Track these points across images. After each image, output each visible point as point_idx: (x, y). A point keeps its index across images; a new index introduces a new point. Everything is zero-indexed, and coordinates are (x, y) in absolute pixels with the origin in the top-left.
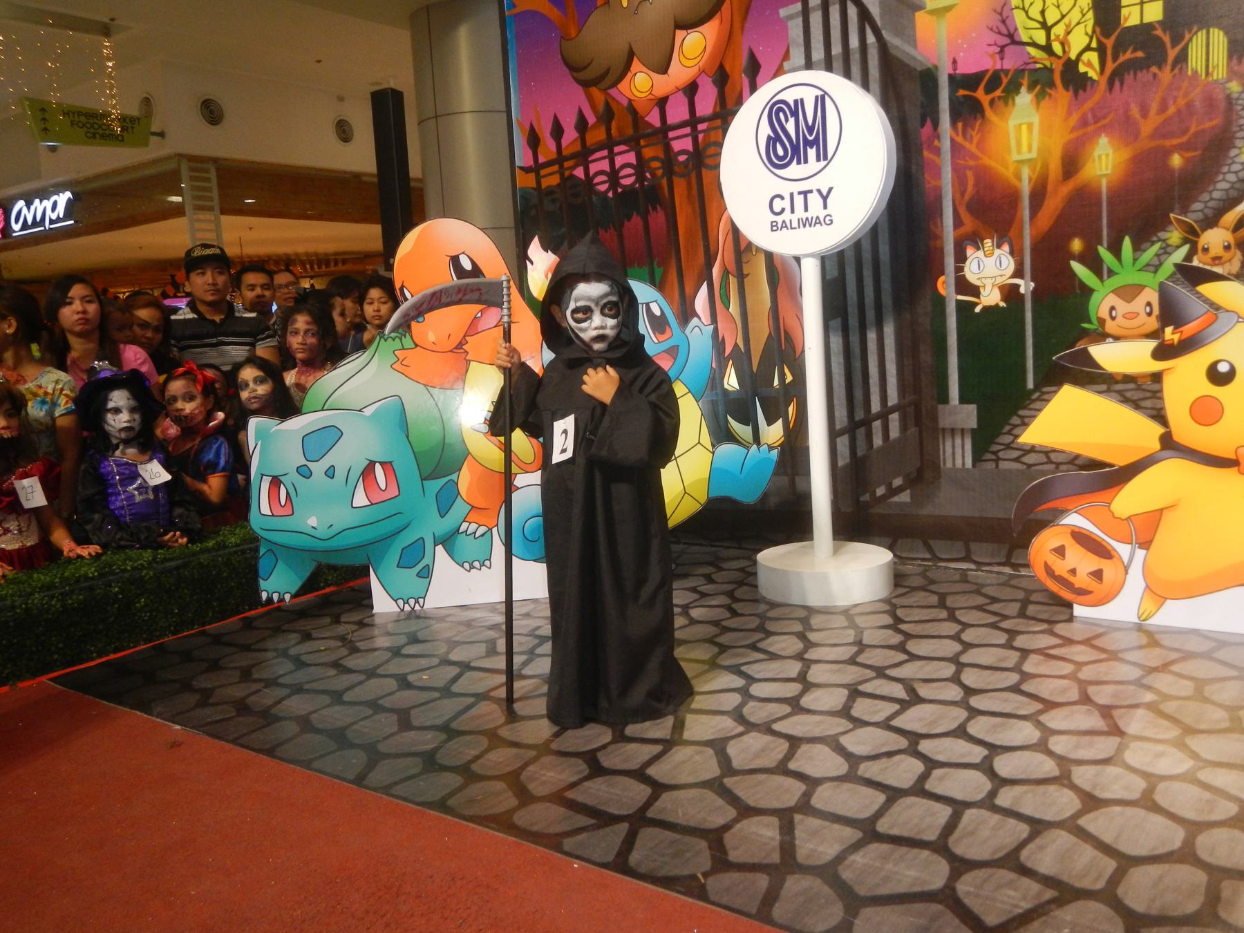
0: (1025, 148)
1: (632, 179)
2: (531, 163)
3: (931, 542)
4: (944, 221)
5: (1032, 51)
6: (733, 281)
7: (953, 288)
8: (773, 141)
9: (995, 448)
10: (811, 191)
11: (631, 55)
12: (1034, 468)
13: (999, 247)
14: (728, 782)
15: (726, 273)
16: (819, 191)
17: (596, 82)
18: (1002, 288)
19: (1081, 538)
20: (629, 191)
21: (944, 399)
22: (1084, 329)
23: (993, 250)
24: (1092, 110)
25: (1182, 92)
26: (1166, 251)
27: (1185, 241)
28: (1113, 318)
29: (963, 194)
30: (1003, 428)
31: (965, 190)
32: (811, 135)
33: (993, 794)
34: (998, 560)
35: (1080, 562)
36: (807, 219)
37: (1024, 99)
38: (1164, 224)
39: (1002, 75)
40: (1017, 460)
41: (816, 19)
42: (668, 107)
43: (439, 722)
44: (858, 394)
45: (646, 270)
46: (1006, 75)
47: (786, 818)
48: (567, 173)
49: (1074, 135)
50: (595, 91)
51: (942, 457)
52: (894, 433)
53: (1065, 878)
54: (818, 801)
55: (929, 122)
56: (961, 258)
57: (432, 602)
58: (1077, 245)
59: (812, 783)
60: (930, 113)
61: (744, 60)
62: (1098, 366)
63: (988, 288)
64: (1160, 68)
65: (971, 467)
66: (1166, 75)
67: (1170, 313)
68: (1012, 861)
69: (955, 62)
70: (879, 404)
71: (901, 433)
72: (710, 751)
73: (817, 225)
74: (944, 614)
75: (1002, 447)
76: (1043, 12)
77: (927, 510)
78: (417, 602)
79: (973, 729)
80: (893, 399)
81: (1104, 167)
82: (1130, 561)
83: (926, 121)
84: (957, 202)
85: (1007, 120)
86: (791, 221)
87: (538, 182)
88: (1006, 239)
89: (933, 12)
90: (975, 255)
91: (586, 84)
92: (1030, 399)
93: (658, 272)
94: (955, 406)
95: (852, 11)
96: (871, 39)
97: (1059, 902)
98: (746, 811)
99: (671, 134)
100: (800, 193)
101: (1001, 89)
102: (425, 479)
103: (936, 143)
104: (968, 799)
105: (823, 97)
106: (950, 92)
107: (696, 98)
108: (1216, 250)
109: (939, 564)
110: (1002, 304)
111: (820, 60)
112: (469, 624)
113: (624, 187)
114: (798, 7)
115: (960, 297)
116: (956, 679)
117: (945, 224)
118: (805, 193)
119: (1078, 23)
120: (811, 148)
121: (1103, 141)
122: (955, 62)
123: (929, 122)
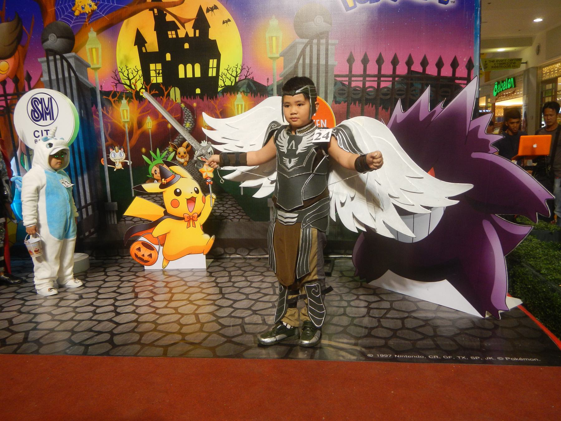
0: (126, 118)
5: (125, 86)
6: (26, 157)
7: (106, 163)
8: (33, 111)
10: (49, 130)
13: (120, 149)
14: (10, 328)
15: (22, 154)
18: (122, 163)
19: (145, 244)
22: (148, 177)
24: (144, 108)
25: (169, 106)
26: (169, 153)
27: (174, 150)
28: (156, 174)
29: (107, 131)
31: (108, 130)
32: (47, 111)
33: (92, 317)
35: (145, 252)
37: (124, 101)
38: (168, 145)
39: (117, 93)
40: (131, 220)
41: (52, 64)
46: (118, 93)
47: (27, 333)
49: (140, 115)
52: (90, 213)
53: (101, 331)
54: (39, 327)
55: (94, 106)
56: (108, 153)
58: (144, 150)
59: (38, 323)
60: (95, 103)
61: (25, 75)
62: (145, 191)
64: (163, 97)
66: (165, 100)
67: (163, 175)
68: (90, 330)
69: (101, 86)
71: (92, 212)
72: (6, 321)
74: (103, 273)
76: (128, 75)
79: (94, 304)
81: (150, 126)
82: (159, 250)
83: (93, 105)
85: (120, 108)
89: (93, 69)
95: (65, 64)
96: (72, 74)
97: (96, 335)
98: (14, 333)
100: (45, 130)
103: (97, 113)
104: (84, 319)
107: (7, 86)
108: (182, 154)
109: (110, 258)
110: (122, 168)
111: (54, 79)
114: (45, 59)
115: (109, 166)
116: (97, 292)
118: (47, 131)
119: (139, 80)
120: (48, 115)
121: (149, 118)
122: (101, 86)
123: (94, 106)
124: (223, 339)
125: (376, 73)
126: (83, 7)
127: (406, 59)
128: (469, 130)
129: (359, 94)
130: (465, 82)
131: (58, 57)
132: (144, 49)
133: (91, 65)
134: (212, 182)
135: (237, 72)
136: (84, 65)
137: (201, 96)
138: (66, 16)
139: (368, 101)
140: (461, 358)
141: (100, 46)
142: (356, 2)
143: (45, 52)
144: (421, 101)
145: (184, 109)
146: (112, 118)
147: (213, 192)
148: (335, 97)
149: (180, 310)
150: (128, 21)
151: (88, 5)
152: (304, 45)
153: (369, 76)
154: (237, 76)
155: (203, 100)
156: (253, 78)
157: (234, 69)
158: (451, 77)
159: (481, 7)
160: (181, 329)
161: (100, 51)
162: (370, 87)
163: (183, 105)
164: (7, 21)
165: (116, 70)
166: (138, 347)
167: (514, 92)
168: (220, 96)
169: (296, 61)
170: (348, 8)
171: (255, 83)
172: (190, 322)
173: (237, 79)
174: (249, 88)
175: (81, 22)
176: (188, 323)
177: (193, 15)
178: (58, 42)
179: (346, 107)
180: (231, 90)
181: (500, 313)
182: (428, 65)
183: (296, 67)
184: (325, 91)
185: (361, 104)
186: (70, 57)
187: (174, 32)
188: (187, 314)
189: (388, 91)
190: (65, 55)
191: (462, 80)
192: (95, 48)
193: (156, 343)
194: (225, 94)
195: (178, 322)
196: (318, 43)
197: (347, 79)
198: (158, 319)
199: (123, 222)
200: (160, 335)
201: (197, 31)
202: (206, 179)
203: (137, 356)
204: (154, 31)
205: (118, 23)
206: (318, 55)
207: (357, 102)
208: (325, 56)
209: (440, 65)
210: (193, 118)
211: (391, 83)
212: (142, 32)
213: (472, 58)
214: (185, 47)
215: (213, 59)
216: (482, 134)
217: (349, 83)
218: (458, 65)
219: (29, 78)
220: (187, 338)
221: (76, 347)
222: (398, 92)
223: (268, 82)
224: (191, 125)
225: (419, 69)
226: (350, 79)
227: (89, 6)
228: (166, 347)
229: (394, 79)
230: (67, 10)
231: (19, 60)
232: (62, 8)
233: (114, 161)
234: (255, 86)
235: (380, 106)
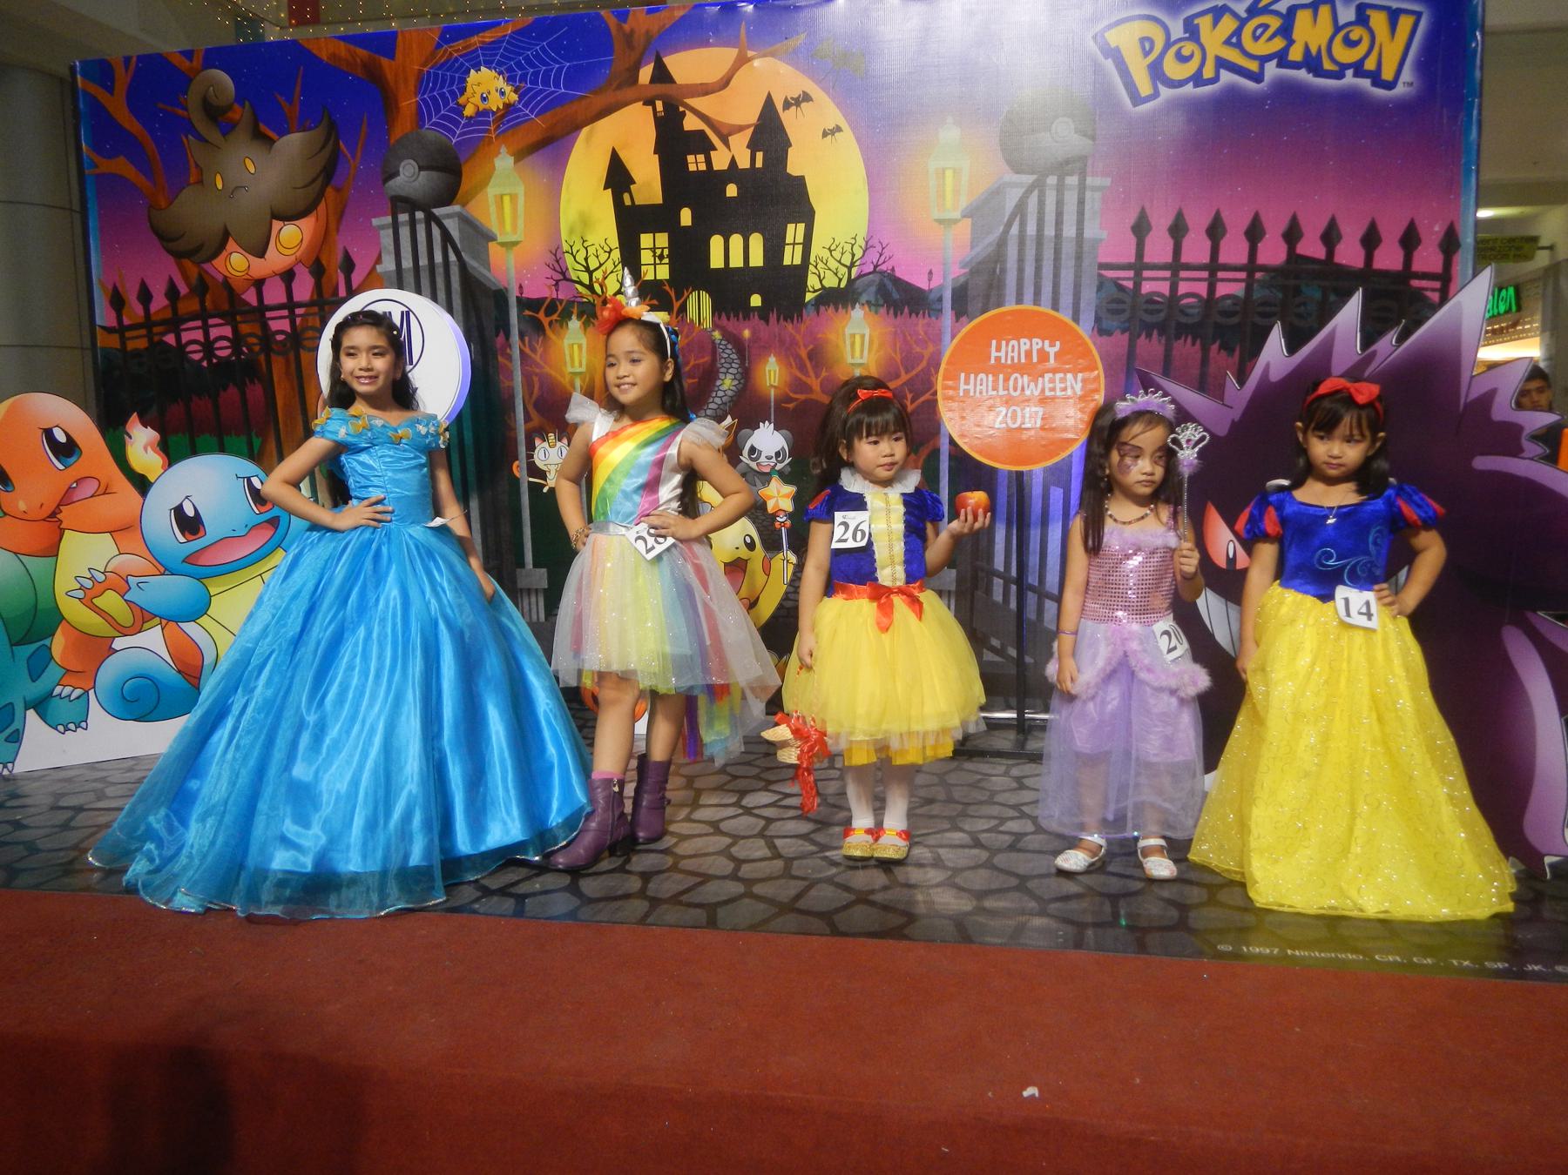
0: (577, 363)
1: (228, 351)
2: (114, 324)
7: (525, 472)
11: (226, 235)
13: (560, 440)
17: (189, 254)
20: (224, 363)
21: (522, 565)
29: (531, 394)
31: (532, 393)
37: (575, 324)
41: (405, 232)
42: (264, 287)
43: (68, 845)
45: (243, 439)
48: (156, 338)
50: (187, 263)
55: (502, 333)
56: (531, 447)
57: (22, 766)
60: (503, 326)
61: (340, 257)
69: (521, 287)
76: (586, 259)
78: (5, 766)
85: (561, 337)
87: (123, 343)
89: (503, 244)
91: (178, 256)
93: (257, 442)
95: (436, 232)
96: (452, 257)
97: (537, 875)
99: (268, 314)
102: (17, 644)
103: (508, 351)
107: (294, 285)
111: (409, 269)
112: (69, 780)
113: (216, 357)
114: (389, 219)
115: (531, 479)
119: (612, 272)
122: (521, 287)
123: (502, 333)
124: (846, 895)
125: (1206, 260)
127: (1283, 226)
128: (1468, 400)
129: (1159, 311)
130: (1437, 285)
131: (420, 215)
132: (626, 197)
134: (788, 523)
135: (853, 255)
136: (480, 236)
137: (763, 313)
139: (1183, 330)
140: (1460, 963)
141: (520, 190)
145: (720, 344)
146: (542, 363)
147: (792, 547)
148: (1098, 320)
149: (724, 826)
150: (591, 132)
152: (1023, 190)
153: (1188, 267)
154: (853, 264)
155: (768, 324)
156: (893, 269)
157: (848, 247)
158: (1399, 272)
159: (1481, 96)
160: (737, 869)
161: (521, 201)
163: (717, 335)
164: (302, 128)
165: (559, 247)
166: (640, 906)
167: (1515, 325)
168: (809, 313)
169: (1001, 228)
170: (1137, 99)
171: (897, 281)
172: (758, 854)
173: (854, 271)
174: (882, 296)
176: (751, 858)
177: (749, 114)
178: (420, 178)
179: (1126, 344)
180: (837, 298)
181: (1552, 866)
182: (1342, 242)
183: (1002, 243)
184: (1073, 304)
185: (1164, 338)
186: (449, 216)
187: (701, 158)
188: (744, 837)
189: (1234, 304)
190: (437, 211)
191: (1429, 279)
192: (511, 195)
193: (684, 898)
194: (822, 308)
195: (725, 852)
196: (1058, 185)
197: (1131, 274)
198: (676, 844)
200: (692, 880)
201: (760, 156)
202: (774, 516)
203: (645, 924)
204: (655, 153)
205: (568, 134)
206: (1059, 215)
207: (1155, 332)
208: (1075, 218)
210: (742, 364)
211: (1243, 285)
212: (622, 155)
214: (728, 195)
215: (796, 223)
216: (1503, 410)
217: (1135, 283)
218: (1419, 241)
219: (349, 265)
220: (758, 889)
221: (495, 899)
222: (1260, 309)
223: (930, 280)
224: (736, 382)
225: (1319, 252)
226: (1138, 274)
228: (711, 909)
229: (1251, 275)
230: (446, 103)
231: (327, 223)
232: (433, 98)
233: (544, 468)
234: (898, 290)
235: (1214, 342)
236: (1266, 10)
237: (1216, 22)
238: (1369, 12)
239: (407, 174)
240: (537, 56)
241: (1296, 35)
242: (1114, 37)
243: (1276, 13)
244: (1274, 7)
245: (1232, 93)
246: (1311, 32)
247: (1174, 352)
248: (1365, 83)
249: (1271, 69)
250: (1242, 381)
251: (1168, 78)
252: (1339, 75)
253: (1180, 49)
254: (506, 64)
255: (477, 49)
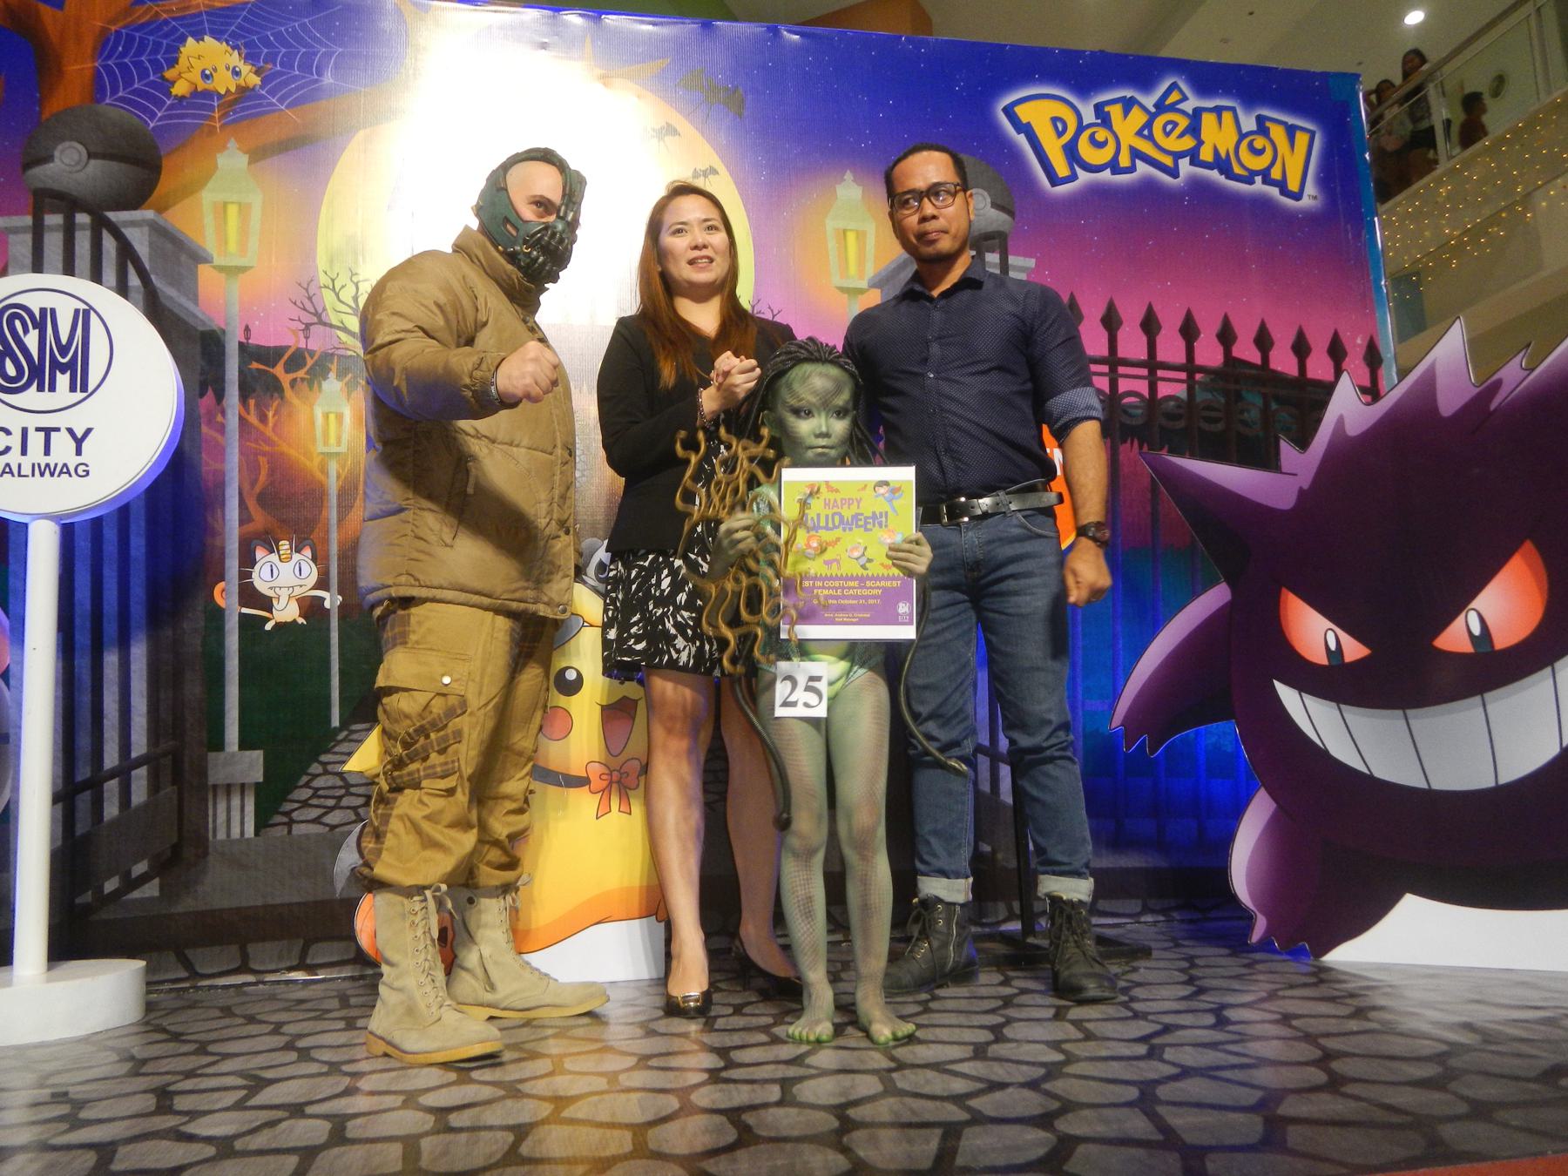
0: (332, 440)
3: (189, 953)
4: (227, 510)
5: (340, 333)
9: (287, 807)
10: (58, 430)
12: (337, 830)
13: (298, 551)
16: (70, 431)
21: (218, 744)
23: (291, 554)
29: (253, 483)
30: (299, 777)
32: (63, 355)
34: (289, 964)
36: (48, 465)
37: (332, 385)
39: (308, 359)
40: (317, 821)
44: (84, 741)
51: (211, 826)
52: (139, 794)
55: (210, 392)
56: (248, 561)
63: (284, 600)
65: (253, 836)
69: (247, 329)
70: (116, 755)
73: (63, 475)
75: (296, 805)
77: (187, 905)
80: (140, 744)
84: (245, 494)
85: (311, 406)
86: (20, 466)
88: (306, 542)
89: (221, 269)
90: (267, 559)
92: (335, 740)
94: (233, 755)
95: (109, 243)
100: (38, 429)
101: (308, 367)
103: (219, 418)
105: (86, 314)
106: (240, 362)
109: (199, 984)
110: (301, 621)
114: (28, 220)
115: (245, 610)
117: (227, 517)
118: (48, 431)
120: (63, 372)
122: (247, 329)
123: (210, 392)
125: (1144, 356)
126: (207, 72)
127: (1217, 326)
133: (215, 256)
138: (135, 92)
141: (256, 200)
142: (1076, 166)
143: (31, 201)
144: (1435, 360)
146: (276, 439)
151: (228, 69)
162: (1129, 393)
170: (1054, 180)
175: (194, 116)
182: (1275, 346)
186: (133, 224)
189: (1179, 407)
190: (113, 216)
199: (280, 828)
209: (1301, 348)
211: (1185, 386)
213: (1375, 339)
218: (1345, 354)
225: (1254, 356)
227: (230, 72)
229: (1191, 376)
230: (143, 74)
232: (124, 68)
233: (270, 593)
236: (1173, 108)
237: (1126, 112)
238: (1268, 124)
239: (67, 161)
240: (295, 35)
241: (1203, 136)
242: (1024, 112)
243: (1183, 113)
244: (1179, 106)
245: (1149, 185)
246: (1218, 136)
247: (1121, 457)
248: (1274, 191)
249: (1184, 165)
250: (1303, 442)
251: (1085, 162)
252: (1251, 182)
253: (1094, 133)
254: (244, 37)
255: (200, 14)
